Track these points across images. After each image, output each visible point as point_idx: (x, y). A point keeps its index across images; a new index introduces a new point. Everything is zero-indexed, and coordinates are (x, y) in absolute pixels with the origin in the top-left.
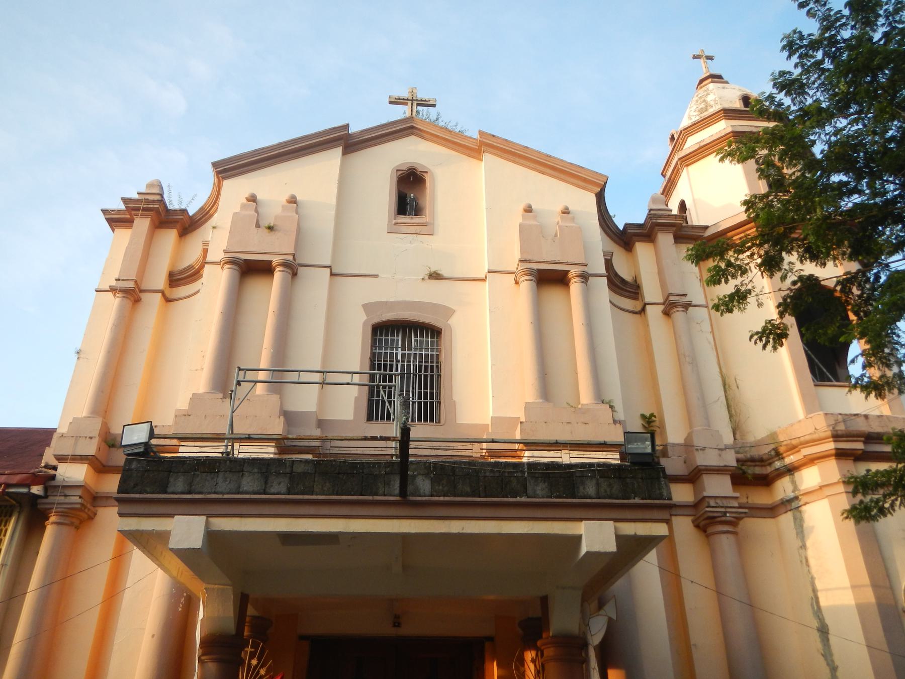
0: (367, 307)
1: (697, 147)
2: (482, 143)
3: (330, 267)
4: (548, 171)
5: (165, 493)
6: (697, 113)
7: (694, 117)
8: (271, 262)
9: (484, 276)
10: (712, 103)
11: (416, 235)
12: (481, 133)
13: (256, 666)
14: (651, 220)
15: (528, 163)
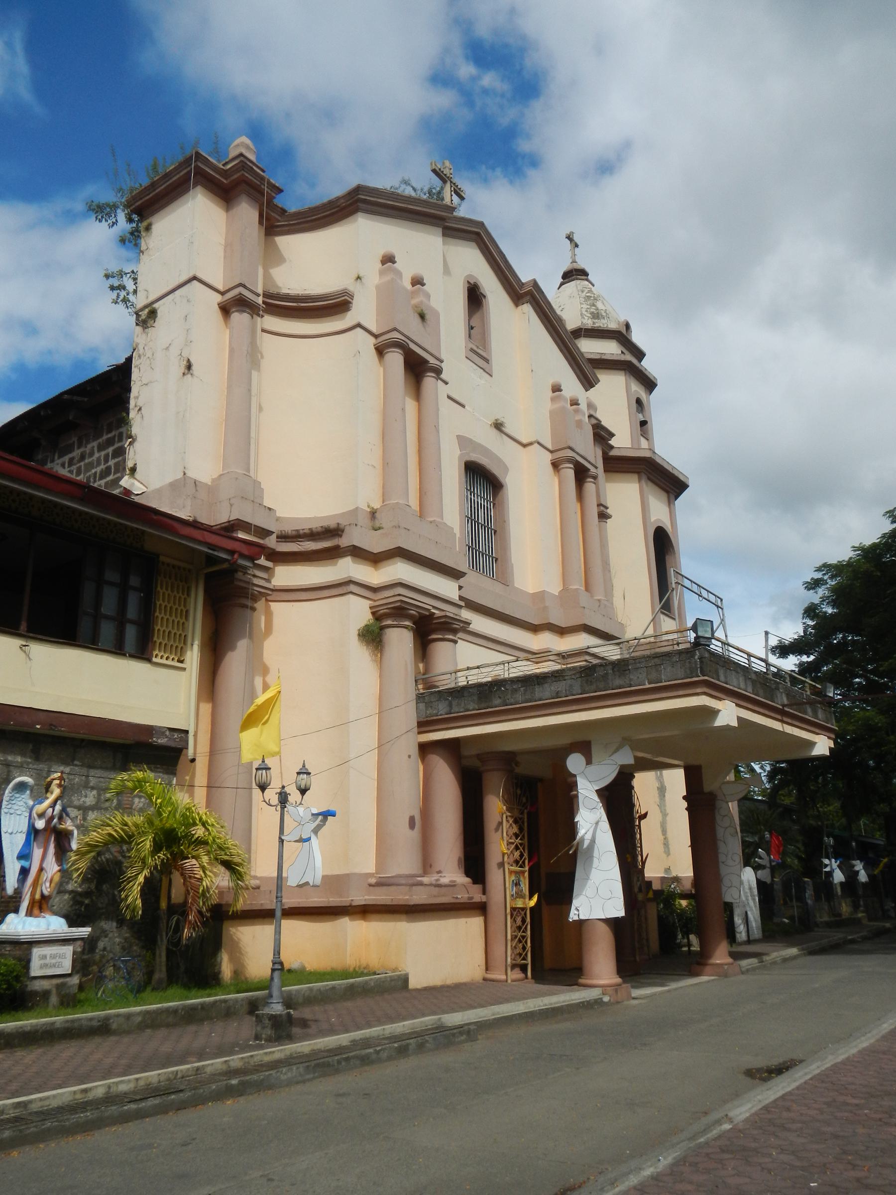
0: (463, 441)
1: (598, 357)
2: (530, 293)
3: (446, 383)
4: (565, 351)
5: (719, 680)
6: (590, 316)
7: (586, 317)
8: (427, 362)
9: (525, 441)
10: (604, 314)
11: (482, 370)
12: (535, 284)
13: (520, 795)
14: (598, 428)
15: (556, 336)
